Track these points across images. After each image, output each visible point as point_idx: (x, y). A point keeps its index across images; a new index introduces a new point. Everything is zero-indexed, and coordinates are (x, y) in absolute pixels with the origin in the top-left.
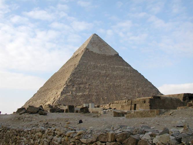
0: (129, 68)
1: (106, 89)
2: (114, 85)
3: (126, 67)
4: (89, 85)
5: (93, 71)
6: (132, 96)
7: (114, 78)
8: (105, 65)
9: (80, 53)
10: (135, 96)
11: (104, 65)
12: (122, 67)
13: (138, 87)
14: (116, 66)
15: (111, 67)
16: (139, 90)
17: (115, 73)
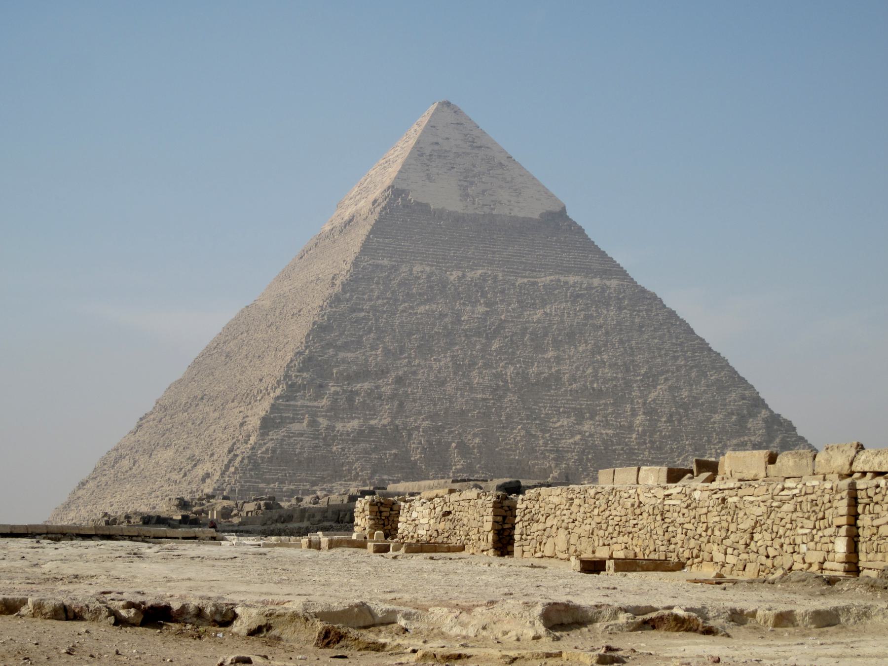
0: (613, 283)
1: (480, 396)
3: (596, 282)
4: (399, 380)
5: (422, 309)
6: (610, 432)
8: (484, 277)
9: (365, 211)
11: (480, 272)
12: (577, 279)
13: (650, 379)
14: (546, 279)
15: (520, 281)
16: (653, 395)
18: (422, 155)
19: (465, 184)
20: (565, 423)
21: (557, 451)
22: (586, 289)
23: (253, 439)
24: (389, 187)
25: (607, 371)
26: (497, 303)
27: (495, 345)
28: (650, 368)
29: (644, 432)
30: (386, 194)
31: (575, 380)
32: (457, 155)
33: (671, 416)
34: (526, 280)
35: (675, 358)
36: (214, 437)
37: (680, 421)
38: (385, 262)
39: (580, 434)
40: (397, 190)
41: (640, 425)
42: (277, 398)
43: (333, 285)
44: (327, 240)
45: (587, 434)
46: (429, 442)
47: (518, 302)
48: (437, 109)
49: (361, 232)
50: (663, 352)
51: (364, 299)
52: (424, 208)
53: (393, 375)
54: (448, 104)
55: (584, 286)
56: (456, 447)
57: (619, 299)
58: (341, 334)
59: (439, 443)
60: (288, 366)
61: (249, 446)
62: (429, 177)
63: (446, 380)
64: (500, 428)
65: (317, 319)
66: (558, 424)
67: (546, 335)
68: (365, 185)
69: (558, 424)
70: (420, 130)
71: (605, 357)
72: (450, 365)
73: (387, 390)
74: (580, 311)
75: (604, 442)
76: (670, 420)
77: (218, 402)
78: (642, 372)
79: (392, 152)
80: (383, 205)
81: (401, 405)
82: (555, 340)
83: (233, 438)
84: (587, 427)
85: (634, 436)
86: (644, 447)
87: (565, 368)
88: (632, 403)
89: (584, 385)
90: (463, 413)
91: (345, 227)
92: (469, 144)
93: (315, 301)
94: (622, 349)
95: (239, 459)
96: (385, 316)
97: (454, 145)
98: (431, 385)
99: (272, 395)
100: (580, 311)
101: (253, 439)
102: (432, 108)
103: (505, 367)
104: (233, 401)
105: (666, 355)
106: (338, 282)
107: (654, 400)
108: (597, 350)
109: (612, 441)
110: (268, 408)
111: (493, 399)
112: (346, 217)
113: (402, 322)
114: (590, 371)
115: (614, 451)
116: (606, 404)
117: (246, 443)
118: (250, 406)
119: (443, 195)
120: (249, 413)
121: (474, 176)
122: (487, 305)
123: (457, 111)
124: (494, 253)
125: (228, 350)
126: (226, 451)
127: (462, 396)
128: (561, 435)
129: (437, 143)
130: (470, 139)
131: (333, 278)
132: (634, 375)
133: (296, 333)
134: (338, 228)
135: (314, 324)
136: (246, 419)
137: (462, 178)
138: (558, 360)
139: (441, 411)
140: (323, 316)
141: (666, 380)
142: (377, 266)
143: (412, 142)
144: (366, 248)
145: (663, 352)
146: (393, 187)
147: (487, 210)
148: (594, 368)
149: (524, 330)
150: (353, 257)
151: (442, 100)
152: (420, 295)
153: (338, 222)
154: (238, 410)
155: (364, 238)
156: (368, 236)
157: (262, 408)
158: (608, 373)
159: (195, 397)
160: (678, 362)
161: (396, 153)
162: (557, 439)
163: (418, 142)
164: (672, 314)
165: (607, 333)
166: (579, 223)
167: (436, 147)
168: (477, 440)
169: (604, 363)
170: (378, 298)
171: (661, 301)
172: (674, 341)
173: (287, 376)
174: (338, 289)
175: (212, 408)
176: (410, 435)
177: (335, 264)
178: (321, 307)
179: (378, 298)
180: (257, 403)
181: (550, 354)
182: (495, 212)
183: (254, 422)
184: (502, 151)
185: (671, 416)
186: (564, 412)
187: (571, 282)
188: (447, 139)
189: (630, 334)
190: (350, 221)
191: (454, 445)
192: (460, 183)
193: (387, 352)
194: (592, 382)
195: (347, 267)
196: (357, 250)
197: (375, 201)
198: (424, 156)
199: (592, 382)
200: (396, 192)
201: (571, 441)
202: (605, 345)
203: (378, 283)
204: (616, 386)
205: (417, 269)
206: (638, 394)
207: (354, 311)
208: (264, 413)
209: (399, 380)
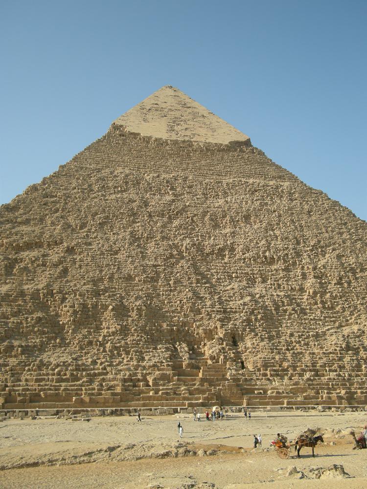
0: (286, 184)
2: (199, 248)
7: (207, 218)
10: (302, 290)
13: (319, 249)
14: (228, 180)
16: (322, 262)
17: (221, 202)
20: (236, 286)
21: (225, 312)
22: (264, 186)
25: (279, 243)
26: (184, 194)
27: (176, 223)
28: (319, 241)
29: (315, 293)
31: (248, 251)
32: (171, 110)
33: (341, 279)
35: (341, 234)
37: (349, 283)
39: (249, 295)
41: (312, 286)
45: (258, 296)
46: (84, 306)
47: (204, 194)
50: (330, 229)
53: (65, 244)
57: (290, 193)
58: (25, 214)
59: (95, 306)
63: (120, 250)
64: (166, 291)
67: (224, 216)
69: (228, 288)
71: (277, 232)
73: (55, 258)
74: (256, 200)
75: (275, 303)
76: (339, 283)
78: (312, 244)
81: (65, 271)
82: (232, 220)
84: (258, 289)
85: (305, 297)
86: (316, 307)
88: (303, 268)
89: (257, 254)
90: (129, 278)
94: (293, 227)
98: (102, 254)
100: (256, 200)
103: (182, 240)
105: (332, 231)
107: (324, 267)
108: (270, 227)
109: (283, 302)
111: (165, 266)
113: (91, 205)
115: (285, 311)
116: (276, 270)
122: (175, 195)
127: (132, 262)
128: (230, 297)
132: (304, 247)
138: (233, 234)
139: (106, 276)
141: (334, 250)
145: (330, 229)
147: (187, 139)
148: (267, 240)
149: (205, 213)
152: (115, 187)
158: (280, 244)
160: (344, 236)
162: (226, 300)
164: (336, 203)
165: (280, 216)
166: (259, 148)
169: (277, 237)
171: (326, 195)
172: (339, 221)
176: (64, 300)
181: (228, 230)
182: (192, 140)
185: (341, 279)
186: (237, 277)
189: (300, 217)
191: (111, 307)
192: (169, 124)
194: (264, 252)
199: (264, 252)
201: (241, 302)
202: (278, 224)
204: (287, 254)
206: (308, 260)
209: (70, 250)
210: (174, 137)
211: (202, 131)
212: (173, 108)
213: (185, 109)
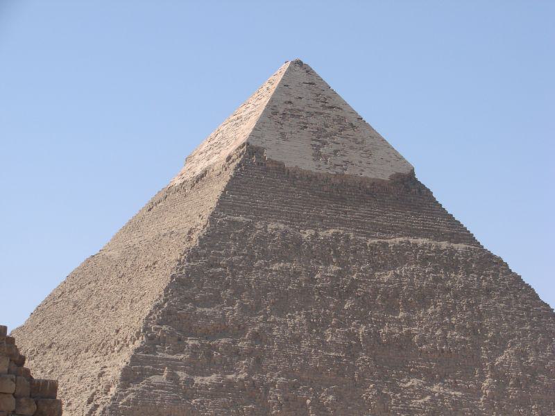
0: (461, 247)
3: (444, 245)
5: (276, 267)
11: (332, 231)
12: (426, 241)
13: (499, 345)
15: (370, 241)
17: (388, 276)
18: (275, 113)
19: (318, 143)
23: (113, 390)
24: (244, 144)
30: (241, 151)
33: (518, 380)
34: (376, 241)
35: (521, 324)
36: (68, 386)
38: (241, 218)
39: (429, 394)
40: (252, 147)
42: (137, 350)
43: (190, 239)
44: (177, 194)
45: (436, 395)
48: (290, 68)
49: (216, 189)
51: (221, 254)
52: (280, 168)
53: (250, 330)
54: (299, 63)
55: (432, 249)
56: (311, 404)
58: (199, 289)
60: (147, 319)
61: (110, 397)
62: (283, 135)
65: (175, 272)
66: (409, 384)
67: (397, 296)
68: (215, 141)
69: (409, 384)
70: (273, 88)
72: (304, 321)
74: (429, 273)
75: (454, 403)
77: (70, 351)
79: (243, 108)
80: (238, 161)
83: (92, 388)
87: (414, 329)
91: (197, 182)
92: (321, 104)
93: (172, 255)
95: (100, 409)
96: (241, 272)
97: (305, 102)
98: (287, 342)
99: (131, 346)
101: (113, 390)
102: (285, 67)
103: (357, 327)
104: (87, 351)
106: (195, 236)
107: (502, 363)
108: (446, 312)
110: (128, 360)
111: (346, 358)
112: (198, 172)
114: (438, 333)
117: (106, 394)
118: (107, 357)
119: (296, 154)
120: (108, 364)
121: (326, 137)
123: (309, 71)
124: (346, 212)
125: (76, 299)
126: (85, 400)
128: (411, 395)
129: (290, 102)
130: (322, 99)
131: (190, 232)
133: (154, 286)
134: (190, 183)
135: (172, 277)
136: (105, 370)
137: (314, 138)
140: (181, 270)
142: (234, 222)
143: (265, 101)
144: (222, 203)
146: (248, 144)
147: (338, 170)
150: (209, 212)
151: (294, 59)
152: (275, 252)
153: (188, 176)
154: (92, 360)
155: (220, 193)
156: (224, 192)
157: (122, 359)
158: (455, 335)
159: (43, 345)
161: (248, 111)
163: (272, 100)
164: (518, 279)
167: (289, 106)
168: (331, 398)
170: (235, 254)
173: (146, 329)
174: (195, 242)
175: (63, 357)
176: (267, 390)
177: (189, 219)
178: (179, 261)
179: (235, 254)
180: (115, 354)
182: (346, 173)
183: (114, 373)
184: (353, 112)
187: (420, 245)
188: (300, 98)
190: (202, 176)
191: (308, 401)
193: (244, 308)
195: (203, 222)
196: (213, 205)
197: (229, 158)
198: (279, 113)
199: (441, 345)
200: (251, 151)
202: (454, 308)
203: (235, 240)
205: (271, 226)
207: (212, 266)
208: (125, 364)
209: (256, 337)
210: (323, 171)
211: (354, 156)
212: (312, 110)
213: (328, 111)
